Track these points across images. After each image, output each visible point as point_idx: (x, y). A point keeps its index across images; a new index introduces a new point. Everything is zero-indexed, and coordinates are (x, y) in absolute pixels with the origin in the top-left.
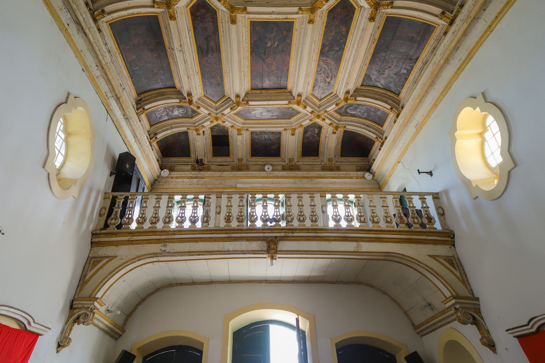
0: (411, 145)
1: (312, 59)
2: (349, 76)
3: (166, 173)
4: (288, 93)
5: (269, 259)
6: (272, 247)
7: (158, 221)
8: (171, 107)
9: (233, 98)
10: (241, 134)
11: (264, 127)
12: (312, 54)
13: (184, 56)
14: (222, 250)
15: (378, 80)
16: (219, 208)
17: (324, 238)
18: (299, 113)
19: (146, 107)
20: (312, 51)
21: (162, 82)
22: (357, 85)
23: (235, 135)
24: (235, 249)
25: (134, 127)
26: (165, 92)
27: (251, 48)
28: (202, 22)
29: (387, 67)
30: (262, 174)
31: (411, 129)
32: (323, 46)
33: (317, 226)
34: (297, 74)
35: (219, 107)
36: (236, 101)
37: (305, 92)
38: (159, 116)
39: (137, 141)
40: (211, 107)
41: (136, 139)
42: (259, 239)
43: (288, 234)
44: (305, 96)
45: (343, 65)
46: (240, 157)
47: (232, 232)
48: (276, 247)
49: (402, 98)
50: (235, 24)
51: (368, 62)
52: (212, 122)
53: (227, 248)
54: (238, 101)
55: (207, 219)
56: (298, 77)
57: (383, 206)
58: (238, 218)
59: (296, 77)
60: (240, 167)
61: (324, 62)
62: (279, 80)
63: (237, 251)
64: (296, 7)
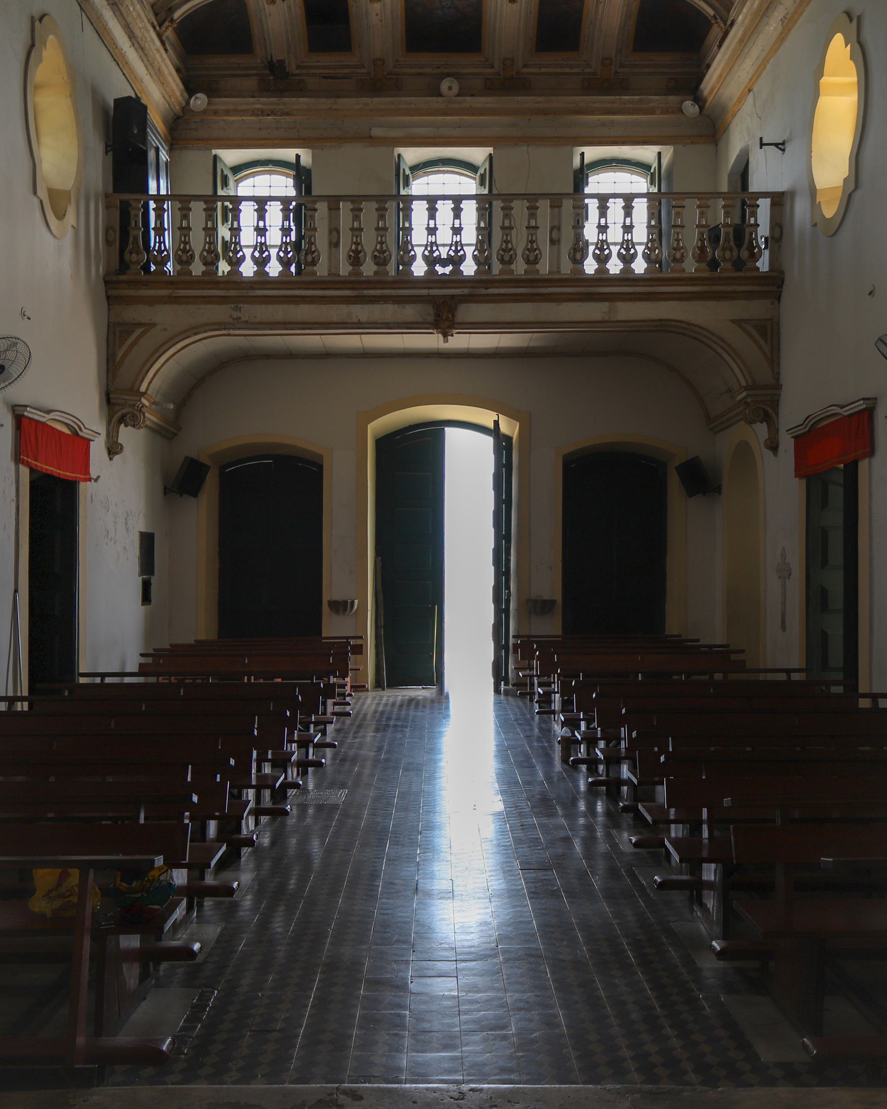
3: (200, 101)
7: (216, 259)
14: (347, 321)
16: (335, 233)
25: (129, 19)
39: (136, 45)
41: (133, 40)
43: (476, 290)
53: (357, 317)
63: (376, 323)
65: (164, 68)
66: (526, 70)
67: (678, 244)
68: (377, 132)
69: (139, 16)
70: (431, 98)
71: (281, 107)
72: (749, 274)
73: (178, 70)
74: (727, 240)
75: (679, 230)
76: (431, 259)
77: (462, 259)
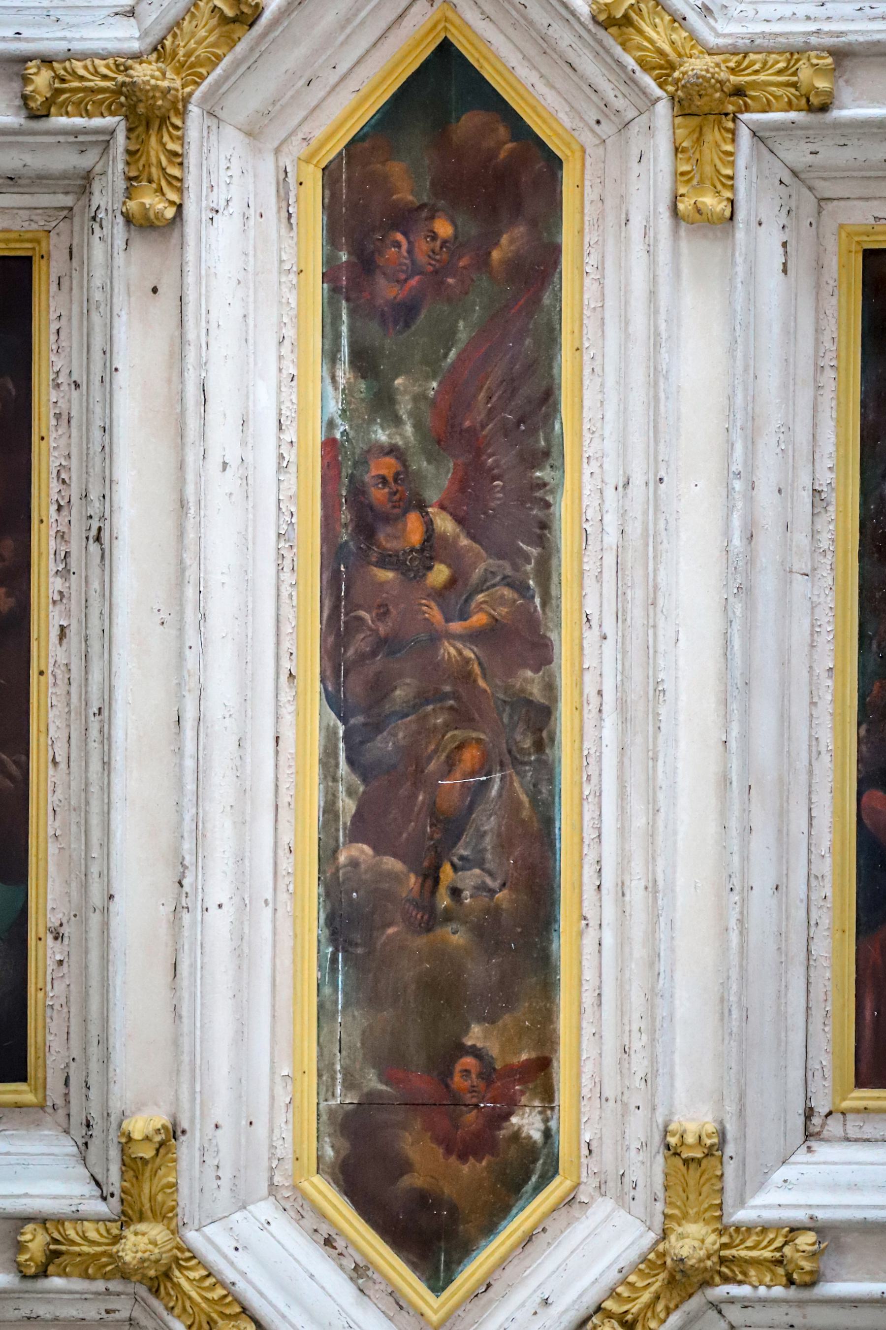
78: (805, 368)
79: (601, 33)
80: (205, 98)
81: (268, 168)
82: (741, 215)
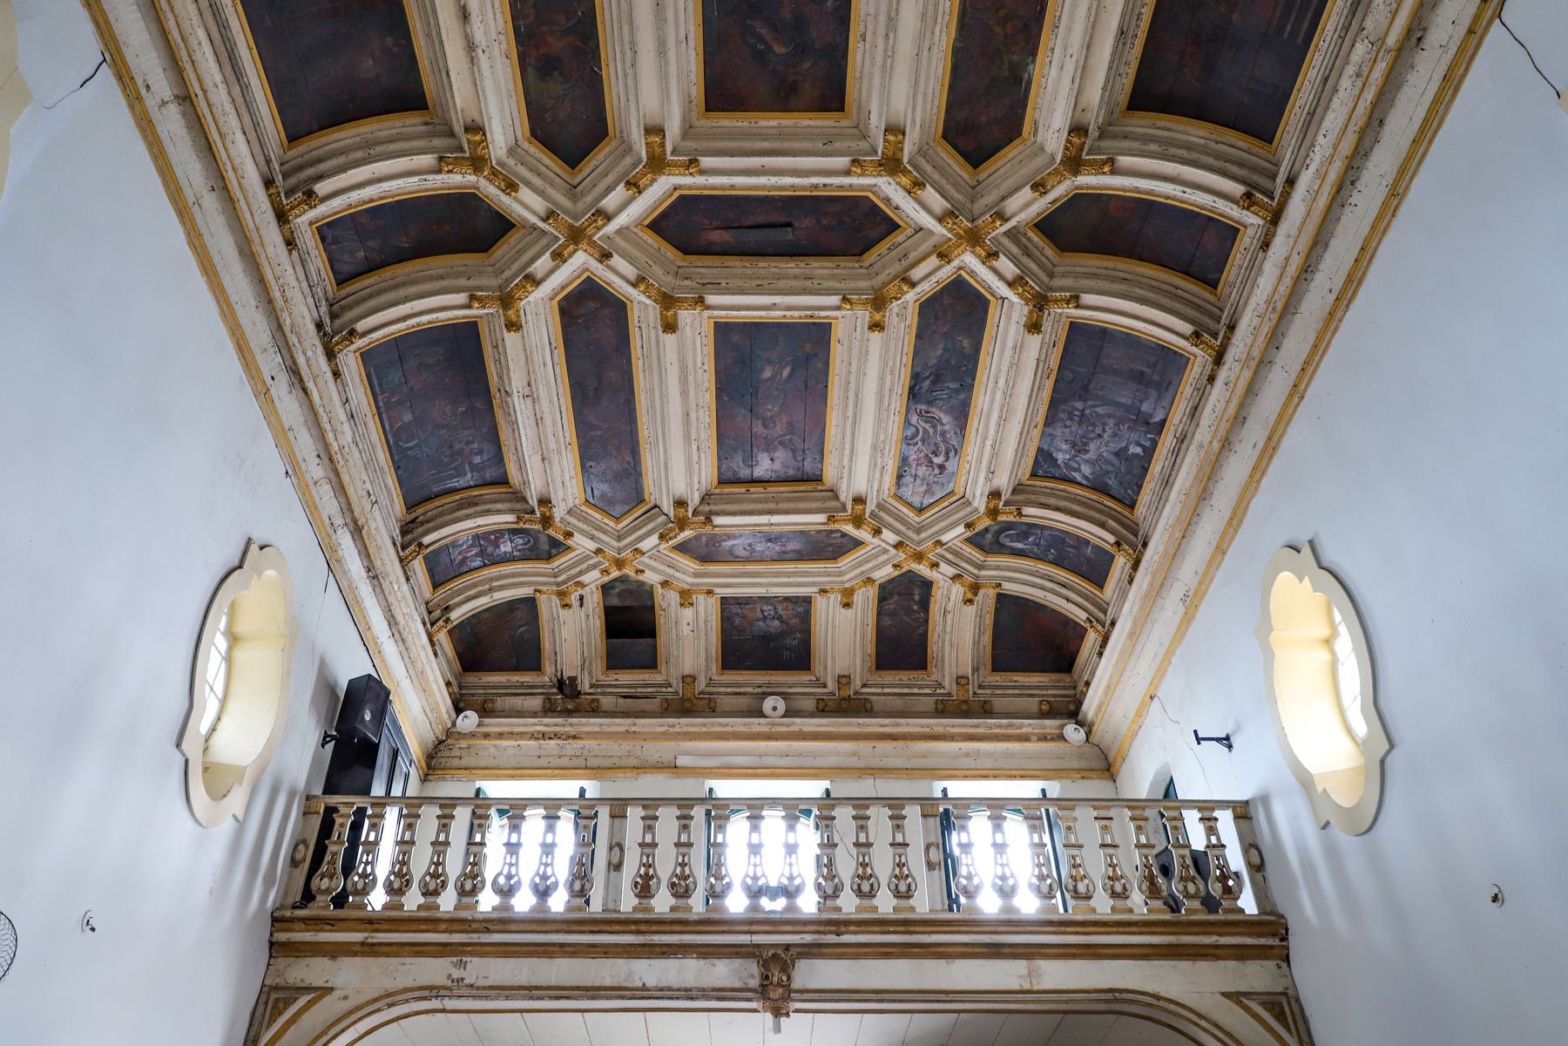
0: (1178, 652)
1: (888, 411)
2: (995, 454)
3: (469, 720)
4: (826, 494)
5: (769, 1016)
6: (775, 979)
8: (494, 532)
9: (667, 507)
10: (692, 604)
11: (760, 585)
12: (886, 400)
13: (537, 408)
14: (626, 984)
15: (1075, 465)
16: (616, 850)
17: (932, 950)
18: (858, 543)
19: (426, 540)
20: (887, 392)
21: (472, 471)
22: (1019, 474)
23: (673, 605)
24: (664, 984)
25: (391, 599)
26: (480, 495)
27: (718, 381)
28: (586, 328)
29: (1093, 435)
30: (756, 725)
31: (1171, 609)
32: (916, 377)
33: (912, 909)
34: (847, 446)
35: (627, 532)
36: (675, 516)
37: (875, 490)
38: (460, 557)
39: (397, 636)
40: (604, 532)
41: (394, 629)
42: (737, 953)
43: (823, 936)
44: (875, 501)
45: (975, 425)
46: (688, 670)
47: (655, 928)
48: (789, 979)
49: (1142, 518)
50: (674, 331)
51: (1041, 419)
52: (606, 571)
53: (641, 979)
54: (681, 515)
55: (583, 886)
56: (852, 453)
57: (1103, 846)
58: (673, 885)
59: (847, 452)
60: (688, 705)
61: (920, 415)
62: (799, 458)
63: (669, 989)
64: (836, 294)
65: (428, 671)
66: (865, 690)
67: (1114, 871)
68: (682, 761)
69: (404, 597)
70: (752, 720)
71: (567, 729)
72: (1231, 917)
73: (448, 684)
74: (1184, 866)
75: (1111, 851)
76: (756, 889)
77: (798, 890)
78: (865, 80)
79: (921, 179)
80: (1053, 164)
81: (1039, 138)
82: (882, 133)
